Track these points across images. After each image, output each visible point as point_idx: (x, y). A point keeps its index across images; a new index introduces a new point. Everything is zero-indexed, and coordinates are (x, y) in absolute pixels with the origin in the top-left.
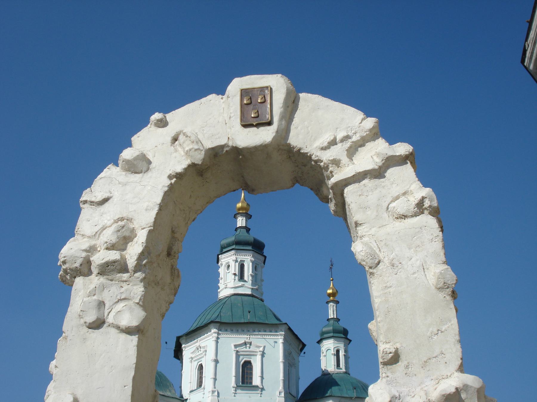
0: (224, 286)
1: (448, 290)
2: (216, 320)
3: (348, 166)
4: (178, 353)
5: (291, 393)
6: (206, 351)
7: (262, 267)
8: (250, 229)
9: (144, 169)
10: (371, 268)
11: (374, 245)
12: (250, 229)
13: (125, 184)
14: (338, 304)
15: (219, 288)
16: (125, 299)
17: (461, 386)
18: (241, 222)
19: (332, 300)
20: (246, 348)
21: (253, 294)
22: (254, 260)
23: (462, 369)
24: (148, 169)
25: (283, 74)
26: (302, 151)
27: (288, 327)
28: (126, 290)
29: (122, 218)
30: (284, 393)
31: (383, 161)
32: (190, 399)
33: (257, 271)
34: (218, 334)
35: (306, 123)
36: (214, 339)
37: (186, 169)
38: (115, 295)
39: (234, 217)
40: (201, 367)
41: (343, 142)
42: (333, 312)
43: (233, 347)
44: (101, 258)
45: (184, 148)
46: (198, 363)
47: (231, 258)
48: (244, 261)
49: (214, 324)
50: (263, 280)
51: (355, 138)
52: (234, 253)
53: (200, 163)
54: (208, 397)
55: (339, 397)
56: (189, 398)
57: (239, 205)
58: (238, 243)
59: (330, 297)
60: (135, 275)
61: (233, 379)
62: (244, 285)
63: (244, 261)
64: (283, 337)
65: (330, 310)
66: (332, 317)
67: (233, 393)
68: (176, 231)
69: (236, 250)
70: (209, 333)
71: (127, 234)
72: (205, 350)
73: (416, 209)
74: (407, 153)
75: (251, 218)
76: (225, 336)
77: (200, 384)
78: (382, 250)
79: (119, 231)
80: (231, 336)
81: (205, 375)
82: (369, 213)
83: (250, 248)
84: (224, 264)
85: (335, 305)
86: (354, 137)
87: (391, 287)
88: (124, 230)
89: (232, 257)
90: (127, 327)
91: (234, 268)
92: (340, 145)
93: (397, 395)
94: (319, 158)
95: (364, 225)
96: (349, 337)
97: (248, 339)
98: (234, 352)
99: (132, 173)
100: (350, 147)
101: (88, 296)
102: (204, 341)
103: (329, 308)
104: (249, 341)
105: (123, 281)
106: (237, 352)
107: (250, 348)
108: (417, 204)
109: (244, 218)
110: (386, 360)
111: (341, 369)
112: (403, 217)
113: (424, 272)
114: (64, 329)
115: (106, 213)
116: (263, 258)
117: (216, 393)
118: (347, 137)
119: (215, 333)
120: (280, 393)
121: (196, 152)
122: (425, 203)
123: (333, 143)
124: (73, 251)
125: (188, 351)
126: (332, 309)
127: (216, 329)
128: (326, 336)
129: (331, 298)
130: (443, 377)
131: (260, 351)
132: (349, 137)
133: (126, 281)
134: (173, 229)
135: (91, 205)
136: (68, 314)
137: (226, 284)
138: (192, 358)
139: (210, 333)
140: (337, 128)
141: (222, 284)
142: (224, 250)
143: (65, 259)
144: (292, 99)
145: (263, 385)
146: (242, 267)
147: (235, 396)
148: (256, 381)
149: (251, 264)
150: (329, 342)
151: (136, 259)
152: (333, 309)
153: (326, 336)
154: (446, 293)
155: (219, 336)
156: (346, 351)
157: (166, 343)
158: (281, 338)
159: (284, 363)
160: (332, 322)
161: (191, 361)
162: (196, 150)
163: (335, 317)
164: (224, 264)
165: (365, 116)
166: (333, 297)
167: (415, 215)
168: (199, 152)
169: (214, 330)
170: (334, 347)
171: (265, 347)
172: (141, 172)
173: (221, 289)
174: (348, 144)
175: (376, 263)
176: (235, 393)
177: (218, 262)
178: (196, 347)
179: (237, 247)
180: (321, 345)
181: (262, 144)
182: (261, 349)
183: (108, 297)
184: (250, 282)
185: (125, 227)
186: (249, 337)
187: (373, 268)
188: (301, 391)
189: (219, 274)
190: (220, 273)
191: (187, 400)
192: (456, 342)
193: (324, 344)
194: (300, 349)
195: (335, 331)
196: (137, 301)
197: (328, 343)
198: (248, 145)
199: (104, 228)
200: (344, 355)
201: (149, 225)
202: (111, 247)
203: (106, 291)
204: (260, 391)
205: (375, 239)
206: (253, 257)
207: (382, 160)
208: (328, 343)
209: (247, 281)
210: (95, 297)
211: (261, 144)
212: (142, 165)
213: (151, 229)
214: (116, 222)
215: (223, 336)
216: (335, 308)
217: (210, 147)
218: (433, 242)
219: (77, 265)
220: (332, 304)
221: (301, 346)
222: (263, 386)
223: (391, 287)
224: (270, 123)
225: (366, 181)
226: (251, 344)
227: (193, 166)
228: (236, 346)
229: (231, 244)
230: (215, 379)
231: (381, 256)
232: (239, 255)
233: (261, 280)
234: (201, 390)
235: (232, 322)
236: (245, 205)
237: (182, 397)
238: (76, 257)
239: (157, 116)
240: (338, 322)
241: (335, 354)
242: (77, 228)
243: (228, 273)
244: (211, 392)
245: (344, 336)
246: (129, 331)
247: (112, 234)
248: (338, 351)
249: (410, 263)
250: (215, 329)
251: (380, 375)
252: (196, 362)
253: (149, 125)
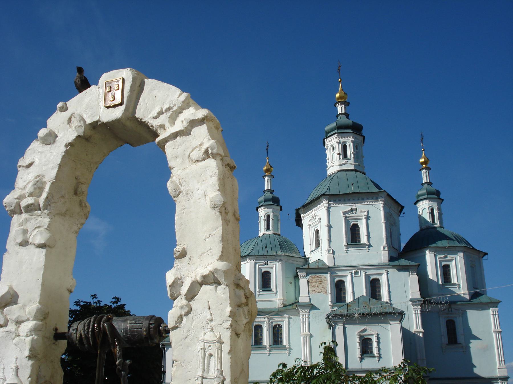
0: (331, 165)
1: (217, 208)
2: (327, 193)
3: (168, 129)
4: (299, 222)
5: (394, 247)
6: (320, 219)
7: (362, 146)
8: (349, 115)
9: (52, 142)
10: (174, 197)
11: (178, 182)
12: (349, 115)
13: (42, 153)
14: (430, 171)
15: (327, 167)
16: (39, 227)
17: (213, 270)
18: (341, 108)
19: (424, 167)
20: (353, 213)
21: (356, 169)
22: (354, 140)
23: (221, 258)
24: (54, 142)
25: (131, 68)
26: (142, 121)
27: (387, 194)
28: (40, 221)
29: (39, 175)
30: (387, 247)
31: (188, 124)
32: (311, 257)
33: (358, 150)
34: (329, 204)
35: (146, 100)
36: (326, 208)
37: (75, 140)
38: (33, 225)
39: (335, 106)
40: (317, 232)
41: (167, 112)
42: (426, 177)
43: (342, 214)
44: (24, 203)
45: (74, 125)
46: (315, 228)
47: (334, 141)
48: (346, 142)
49: (325, 197)
50: (363, 156)
51: (175, 108)
53: (82, 135)
54: (325, 255)
55: (435, 247)
56: (310, 257)
57: (338, 95)
58: (339, 127)
59: (423, 165)
60: (44, 212)
61: (344, 239)
62: (348, 162)
63: (346, 142)
64: (383, 202)
65: (423, 175)
66: (426, 182)
67: (345, 250)
68: (78, 178)
69: (338, 134)
70: (321, 204)
71: (40, 186)
72: (319, 218)
73: (204, 155)
74: (203, 117)
75: (349, 105)
76: (334, 205)
77: (318, 245)
78: (182, 185)
79: (35, 184)
80: (339, 205)
81: (321, 238)
82: (178, 160)
83: (350, 131)
84: (329, 146)
85: (427, 171)
86: (174, 107)
87: (185, 209)
88: (38, 183)
89: (336, 140)
90: (38, 244)
91: (338, 149)
92: (165, 114)
93: (179, 277)
94: (152, 125)
95: (174, 168)
96: (441, 197)
97: (354, 206)
98: (343, 218)
99: (46, 145)
100: (172, 115)
101: (19, 227)
102: (318, 210)
103: (423, 174)
105: (38, 216)
106: (346, 217)
107: (356, 213)
108: (205, 152)
109: (343, 106)
110: (177, 256)
111: (436, 224)
112: (197, 161)
113: (205, 197)
114: (7, 247)
115: (31, 173)
116: (362, 138)
117: (331, 252)
118: (169, 109)
119: (326, 203)
120: (384, 248)
121: (80, 127)
122: (209, 151)
123: (161, 113)
124: (10, 199)
125: (306, 219)
126: (425, 175)
127: (327, 200)
128: (421, 198)
129: (424, 166)
130: (209, 264)
131: (364, 216)
132: (171, 108)
133: (40, 216)
134: (77, 177)
135: (23, 168)
136: (9, 238)
137: (332, 163)
138: (310, 225)
139: (320, 205)
140: (164, 103)
141: (330, 163)
142: (329, 135)
143: (6, 204)
144: (138, 83)
145: (370, 242)
146: (345, 147)
147: (347, 253)
148: (364, 239)
149: (352, 143)
150: (425, 203)
151: (43, 202)
152: (426, 175)
153: (421, 198)
154: (216, 210)
155: (330, 206)
156: (439, 209)
157: (288, 215)
158: (381, 203)
159: (385, 223)
160: (425, 185)
161: (309, 228)
162: (79, 126)
163: (428, 181)
164: (329, 146)
165: (182, 92)
166: (425, 165)
167: (203, 160)
168: (81, 128)
169: (325, 201)
170: (429, 206)
171: (368, 212)
172: (50, 144)
173: (329, 167)
174: (169, 114)
175: (177, 194)
176: (347, 251)
177: (324, 145)
179: (339, 131)
180: (417, 205)
181: (116, 119)
182: (366, 213)
183: (29, 226)
184: (352, 159)
185: (39, 182)
186: (355, 204)
187: (176, 197)
188: (403, 245)
189: (326, 154)
190: (327, 154)
191: (309, 258)
192: (220, 242)
193: (420, 204)
194: (399, 210)
195: (429, 193)
196: (46, 228)
197: (423, 203)
198: (108, 120)
199: (29, 183)
200: (438, 213)
201: (53, 179)
202: (31, 195)
203: (28, 223)
204: (367, 247)
205: (179, 178)
206: (353, 138)
207: (187, 123)
208: (423, 203)
209: (350, 158)
210: (22, 227)
211: (115, 119)
212: (51, 139)
213: (54, 181)
214: (36, 178)
215: (333, 206)
216: (427, 174)
217: (89, 123)
218: (213, 177)
219: (12, 208)
220: (424, 170)
221: (400, 208)
222: (369, 243)
223: (185, 209)
224: (121, 104)
225: (178, 138)
226: (356, 210)
227: (78, 137)
228: (344, 213)
229: (334, 129)
230: (330, 241)
231: (182, 188)
232: (341, 138)
233: (362, 156)
234: (319, 250)
235: (339, 194)
236: (343, 95)
237: (305, 257)
238: (12, 203)
239: (60, 104)
240: (432, 185)
241: (429, 212)
242: (15, 183)
243: (333, 153)
244: (327, 251)
245: (437, 197)
246: (41, 246)
247: (30, 187)
248: (432, 210)
249: (198, 192)
250: (326, 201)
251: (174, 265)
252: (314, 228)
253: (57, 111)
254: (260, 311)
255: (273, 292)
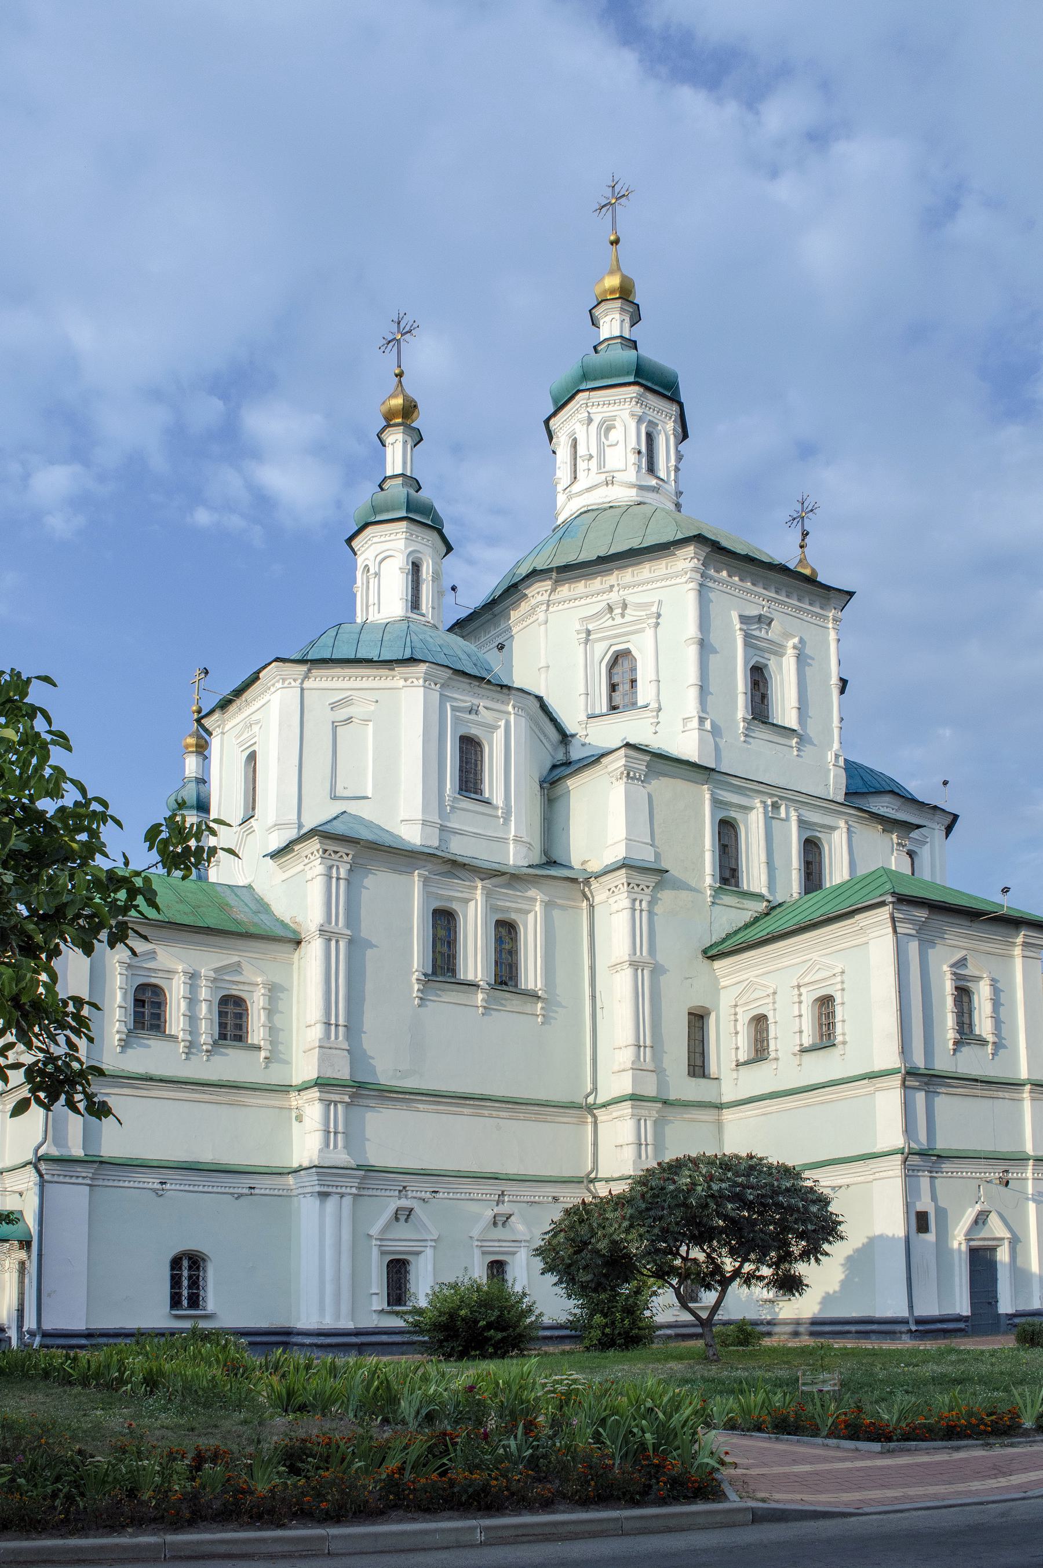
40: (620, 659)
48: (657, 425)
52: (635, 395)
84: (597, 419)
104: (768, 615)
117: (708, 725)
161: (587, 641)
176: (746, 736)
178: (604, 604)
182: (796, 640)
243: (608, 446)
252: (604, 644)
254: (460, 859)
255: (496, 808)
